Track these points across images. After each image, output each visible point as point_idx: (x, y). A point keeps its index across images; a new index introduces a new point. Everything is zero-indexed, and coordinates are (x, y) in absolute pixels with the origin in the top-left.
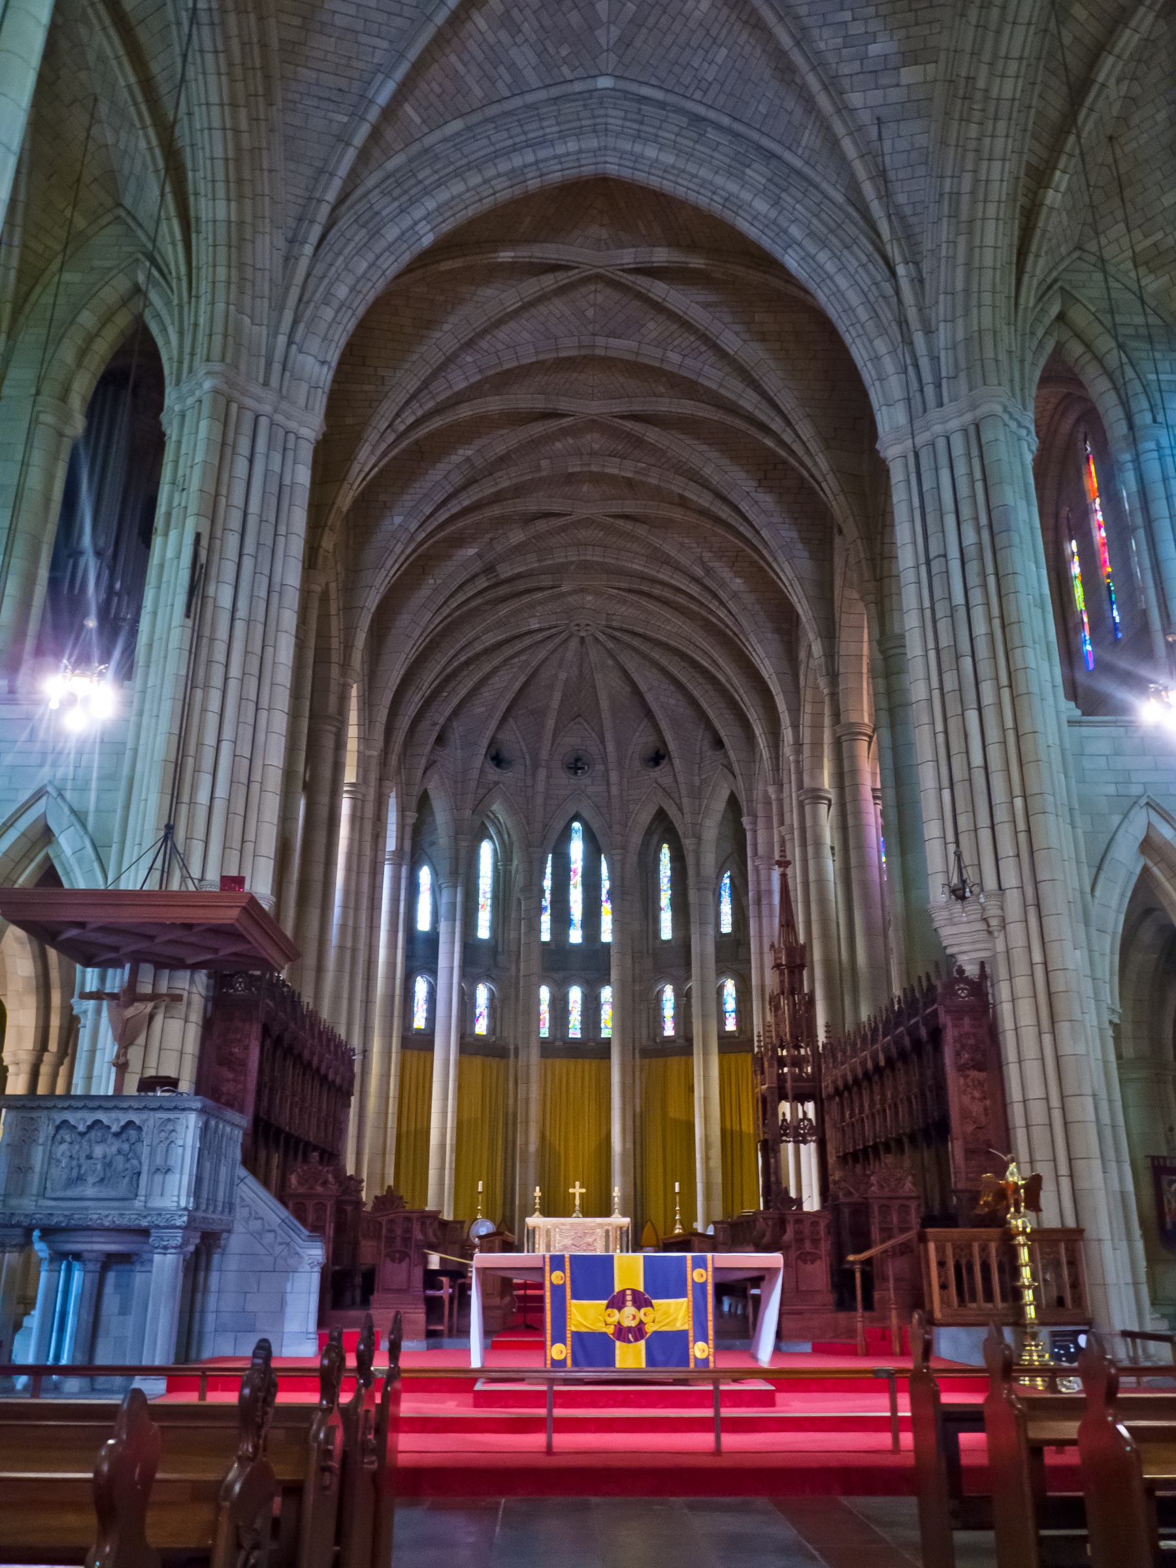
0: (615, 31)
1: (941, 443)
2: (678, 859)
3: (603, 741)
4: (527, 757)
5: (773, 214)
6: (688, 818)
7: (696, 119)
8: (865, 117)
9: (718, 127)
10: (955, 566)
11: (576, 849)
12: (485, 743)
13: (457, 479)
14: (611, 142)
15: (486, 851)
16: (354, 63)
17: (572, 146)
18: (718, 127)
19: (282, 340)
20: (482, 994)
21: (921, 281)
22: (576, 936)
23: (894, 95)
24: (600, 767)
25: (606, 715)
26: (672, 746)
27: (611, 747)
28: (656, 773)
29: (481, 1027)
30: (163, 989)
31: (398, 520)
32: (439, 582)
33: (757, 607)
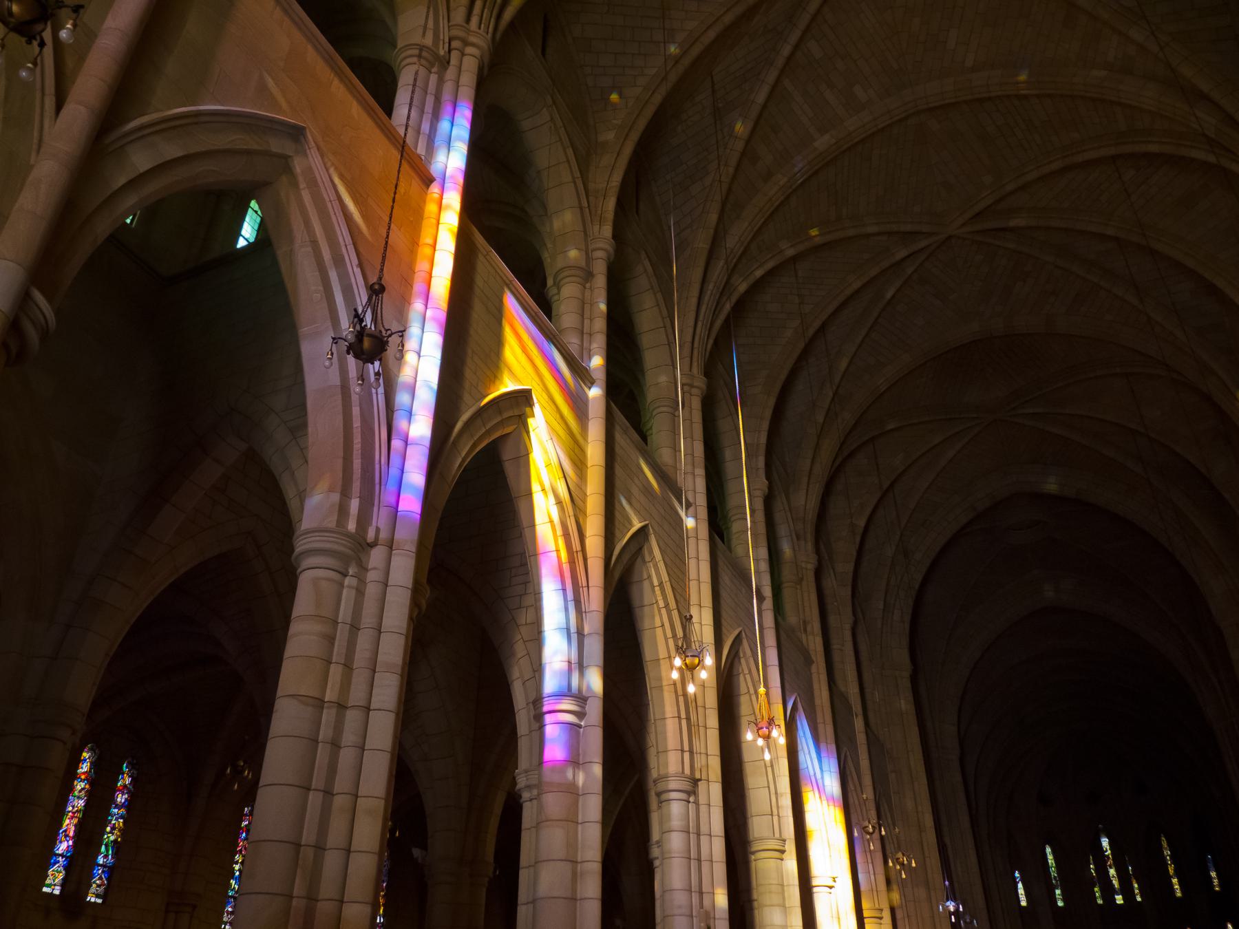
11: (1105, 842)
15: (1048, 850)
22: (1119, 900)
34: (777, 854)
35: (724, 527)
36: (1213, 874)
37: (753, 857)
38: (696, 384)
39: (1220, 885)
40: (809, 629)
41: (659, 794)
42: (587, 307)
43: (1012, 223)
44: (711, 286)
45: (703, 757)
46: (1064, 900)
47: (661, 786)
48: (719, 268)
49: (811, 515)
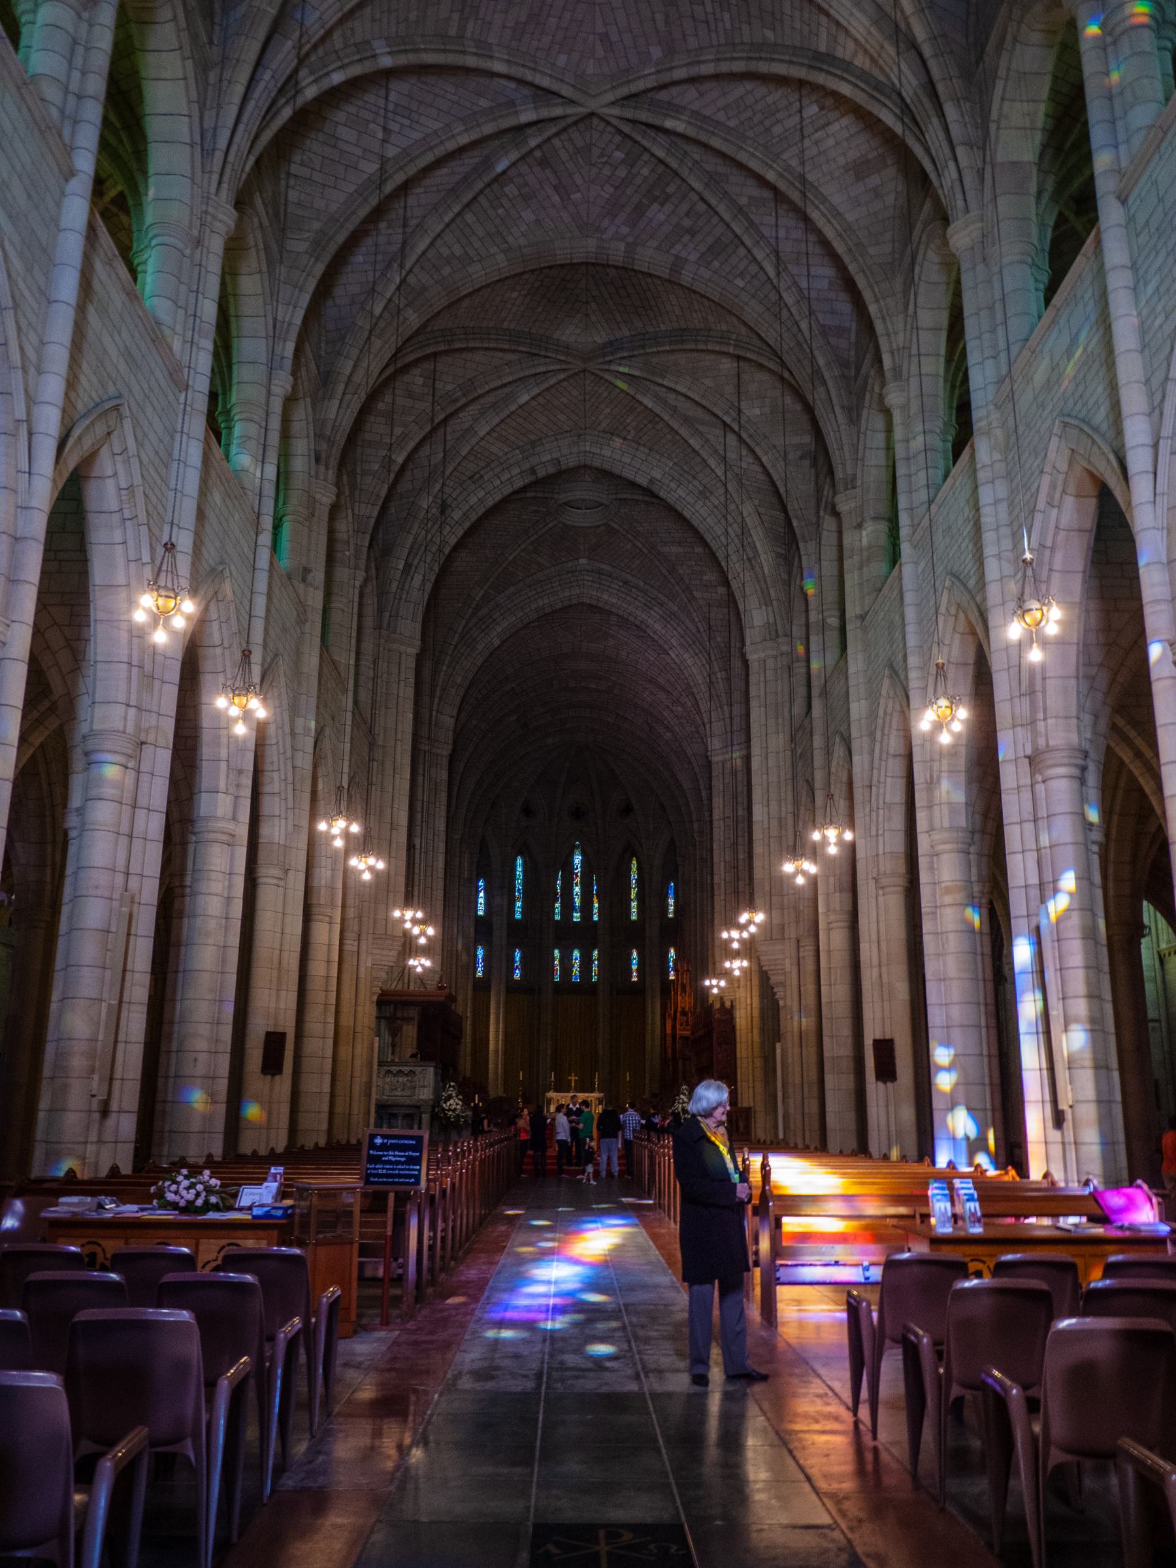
7: (626, 583)
11: (577, 860)
15: (519, 861)
17: (567, 594)
20: (518, 955)
22: (577, 917)
29: (517, 975)
30: (405, 1014)
31: (474, 722)
34: (225, 838)
35: (223, 425)
36: (671, 901)
37: (194, 838)
38: (221, 216)
39: (675, 912)
40: (310, 577)
41: (87, 754)
42: (80, 50)
43: (669, 124)
44: (267, 75)
45: (154, 716)
46: (522, 913)
47: (91, 745)
48: (283, 56)
49: (341, 438)
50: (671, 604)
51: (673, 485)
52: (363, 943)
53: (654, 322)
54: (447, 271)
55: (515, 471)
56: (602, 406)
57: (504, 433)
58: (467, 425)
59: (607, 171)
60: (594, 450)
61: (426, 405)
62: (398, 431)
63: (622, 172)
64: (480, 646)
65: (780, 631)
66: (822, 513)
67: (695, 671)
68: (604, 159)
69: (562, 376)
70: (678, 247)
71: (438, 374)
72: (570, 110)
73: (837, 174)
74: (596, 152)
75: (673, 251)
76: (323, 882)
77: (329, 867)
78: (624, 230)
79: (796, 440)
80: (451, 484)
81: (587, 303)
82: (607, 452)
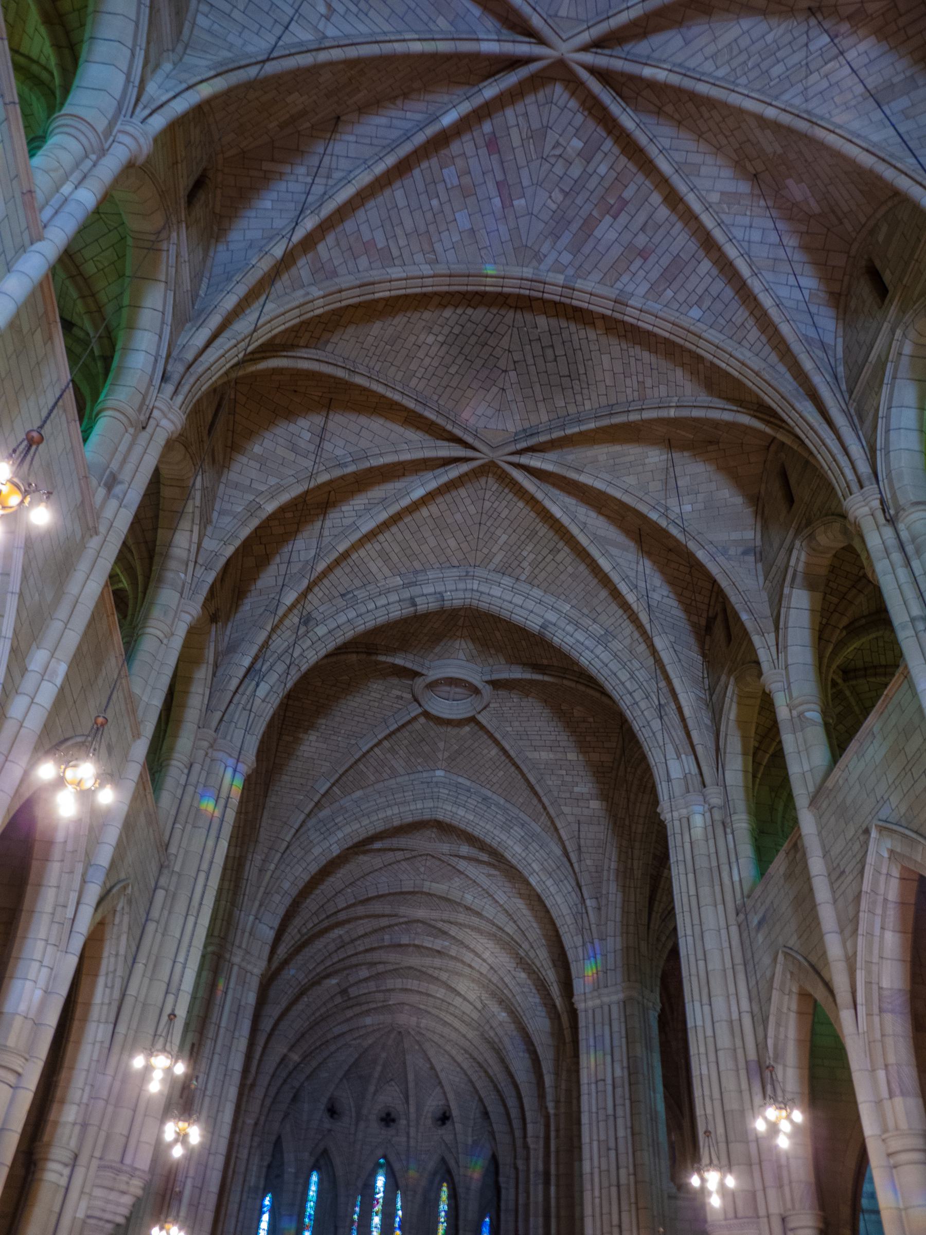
0: (446, 754)
1: (606, 1008)
2: (453, 1196)
3: (407, 1102)
4: (353, 1109)
5: (524, 855)
6: (462, 1171)
7: (485, 799)
8: (570, 819)
9: (497, 805)
10: (609, 1088)
11: (380, 1181)
12: (324, 1100)
13: (332, 947)
14: (440, 805)
15: (314, 1178)
16: (311, 772)
17: (419, 806)
18: (497, 805)
19: (251, 918)
21: (599, 909)
23: (586, 812)
24: (403, 1122)
25: (411, 1085)
26: (455, 1113)
27: (412, 1109)
28: (441, 1131)
31: (292, 972)
32: (311, 1000)
33: (515, 1033)
40: (118, 489)
50: (533, 824)
51: (570, 629)
52: (80, 1172)
53: (579, 397)
54: (363, 262)
55: (393, 597)
56: (499, 532)
57: (385, 545)
58: (347, 522)
59: (559, 169)
60: (482, 589)
61: (308, 463)
62: (272, 481)
63: (576, 171)
64: (317, 851)
65: (708, 780)
66: (786, 591)
67: (559, 899)
68: (558, 152)
69: (464, 468)
70: (625, 278)
71: (328, 436)
72: (538, 50)
73: (853, 103)
74: (552, 137)
75: (619, 285)
76: (22, 1008)
77: (42, 983)
78: (566, 258)
79: (735, 536)
80: (320, 594)
81: (506, 371)
82: (496, 591)
